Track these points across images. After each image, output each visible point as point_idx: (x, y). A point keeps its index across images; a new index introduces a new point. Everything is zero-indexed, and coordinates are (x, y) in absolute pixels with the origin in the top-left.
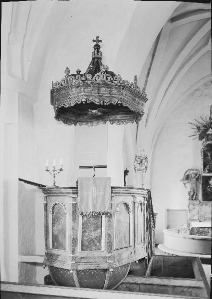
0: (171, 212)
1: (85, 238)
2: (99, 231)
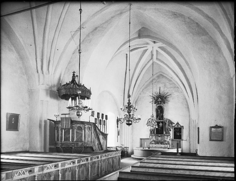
0: (143, 140)
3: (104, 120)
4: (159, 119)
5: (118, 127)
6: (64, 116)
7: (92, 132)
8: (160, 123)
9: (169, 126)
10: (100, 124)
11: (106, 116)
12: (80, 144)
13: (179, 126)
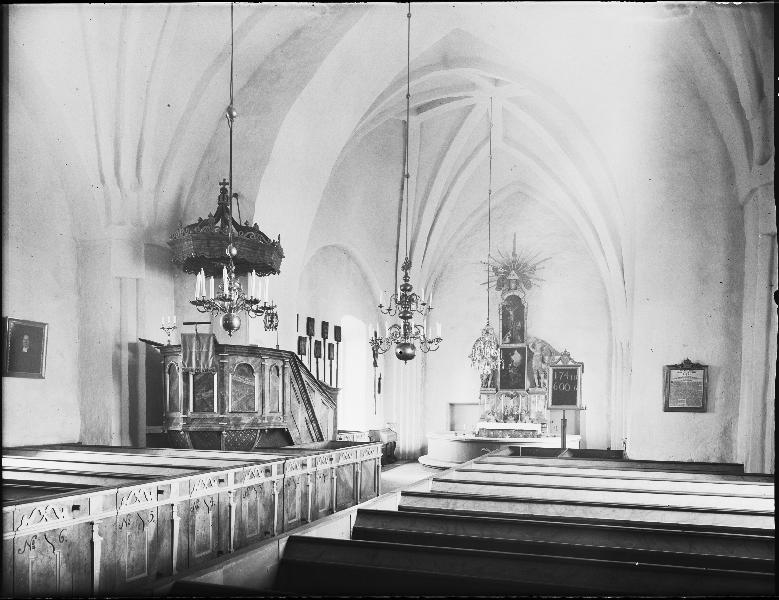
0: (456, 407)
2: (210, 392)
3: (330, 344)
4: (512, 341)
5: (375, 364)
6: (190, 330)
7: (287, 381)
8: (513, 354)
9: (543, 361)
10: (318, 356)
11: (338, 330)
12: (246, 420)
13: (570, 363)
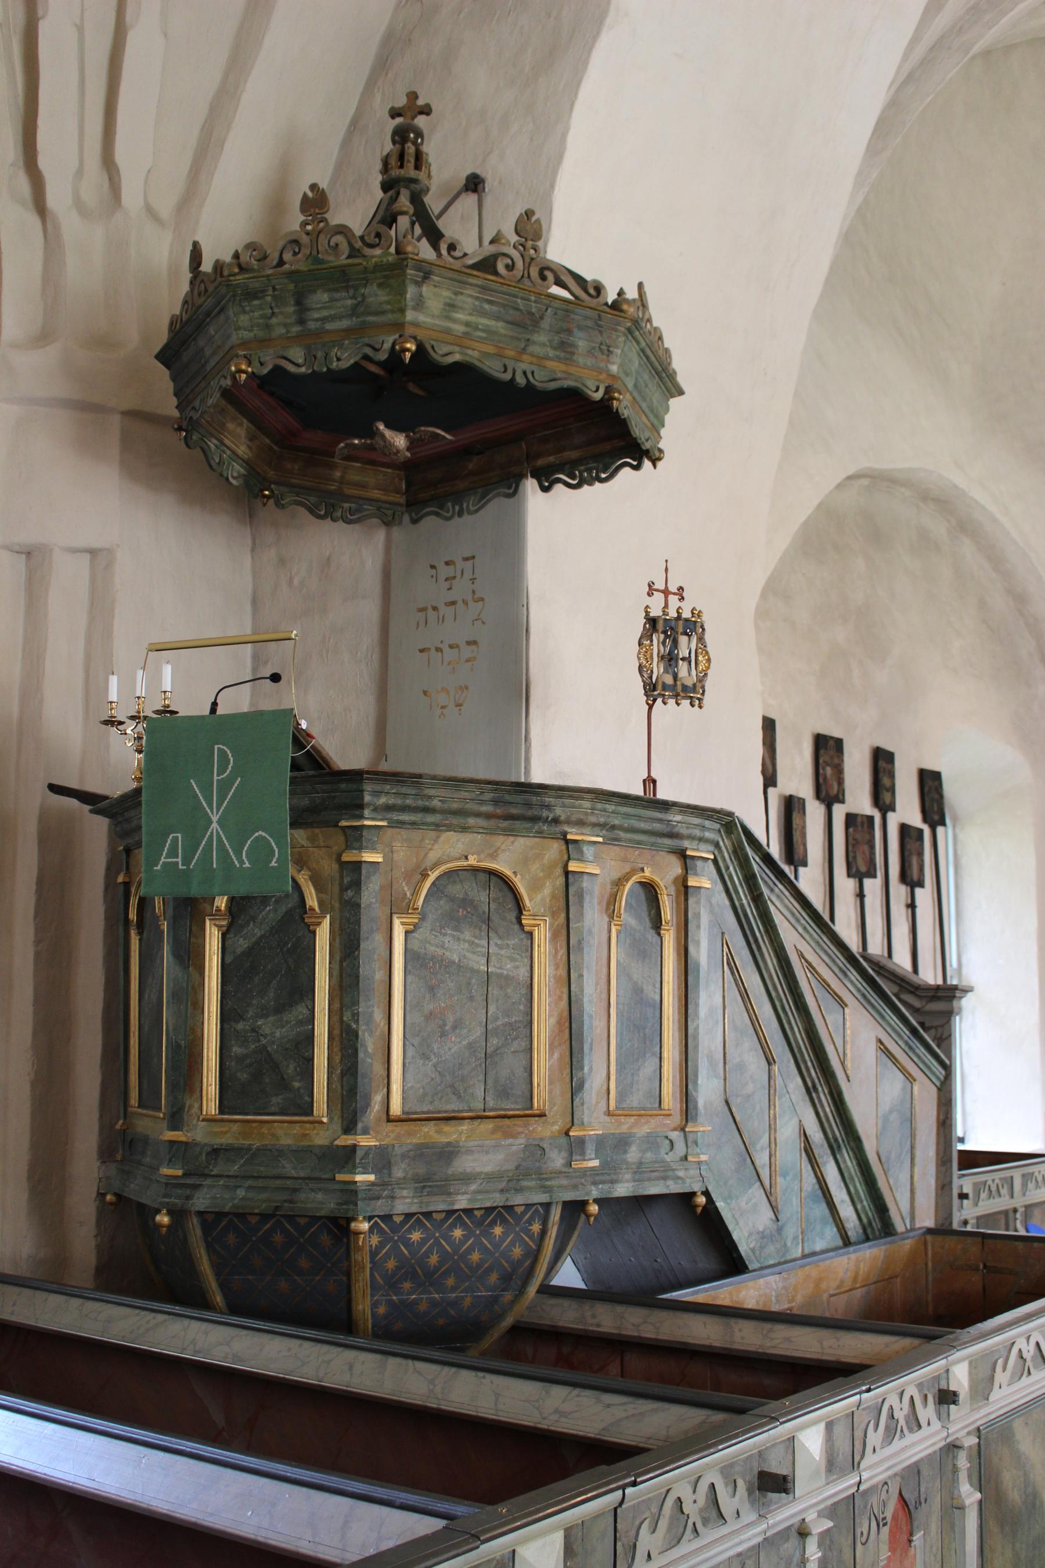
1: (237, 1050)
2: (301, 1010)
7: (703, 951)
10: (860, 871)
